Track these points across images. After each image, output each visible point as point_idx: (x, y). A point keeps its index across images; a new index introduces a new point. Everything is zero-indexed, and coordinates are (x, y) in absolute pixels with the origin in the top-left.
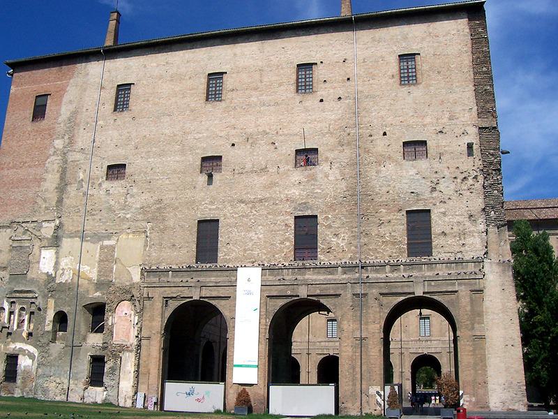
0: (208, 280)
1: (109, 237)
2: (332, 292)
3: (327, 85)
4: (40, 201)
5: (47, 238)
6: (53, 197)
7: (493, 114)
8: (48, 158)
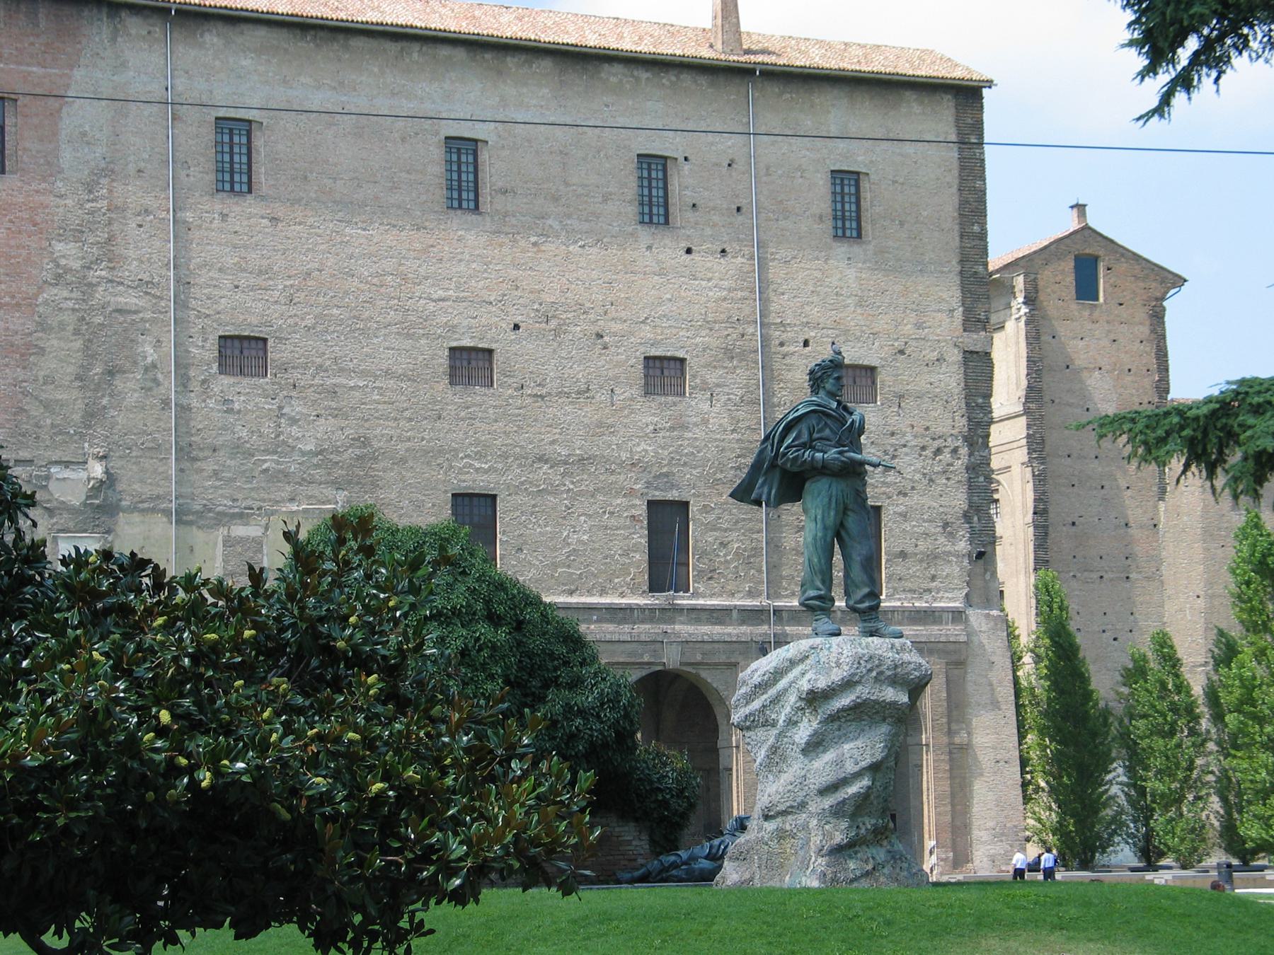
1: (243, 517)
2: (723, 659)
6: (72, 399)
8: (41, 289)
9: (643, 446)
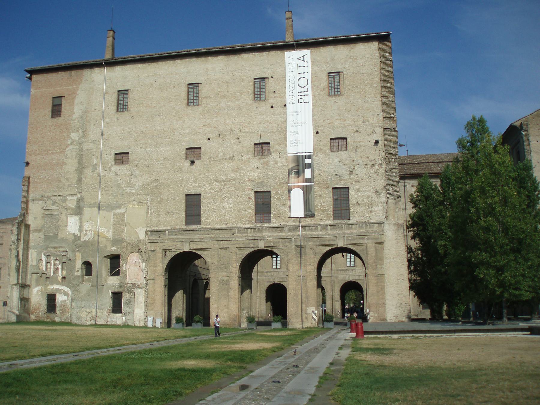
0: (195, 237)
1: (119, 207)
2: (281, 245)
3: (276, 95)
4: (63, 180)
5: (72, 208)
6: (74, 177)
7: (394, 119)
8: (67, 147)
9: (253, 173)
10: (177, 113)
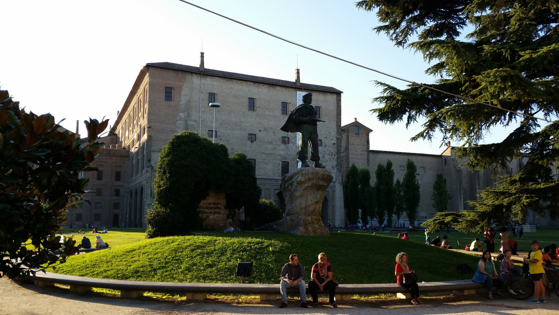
10: (243, 113)
